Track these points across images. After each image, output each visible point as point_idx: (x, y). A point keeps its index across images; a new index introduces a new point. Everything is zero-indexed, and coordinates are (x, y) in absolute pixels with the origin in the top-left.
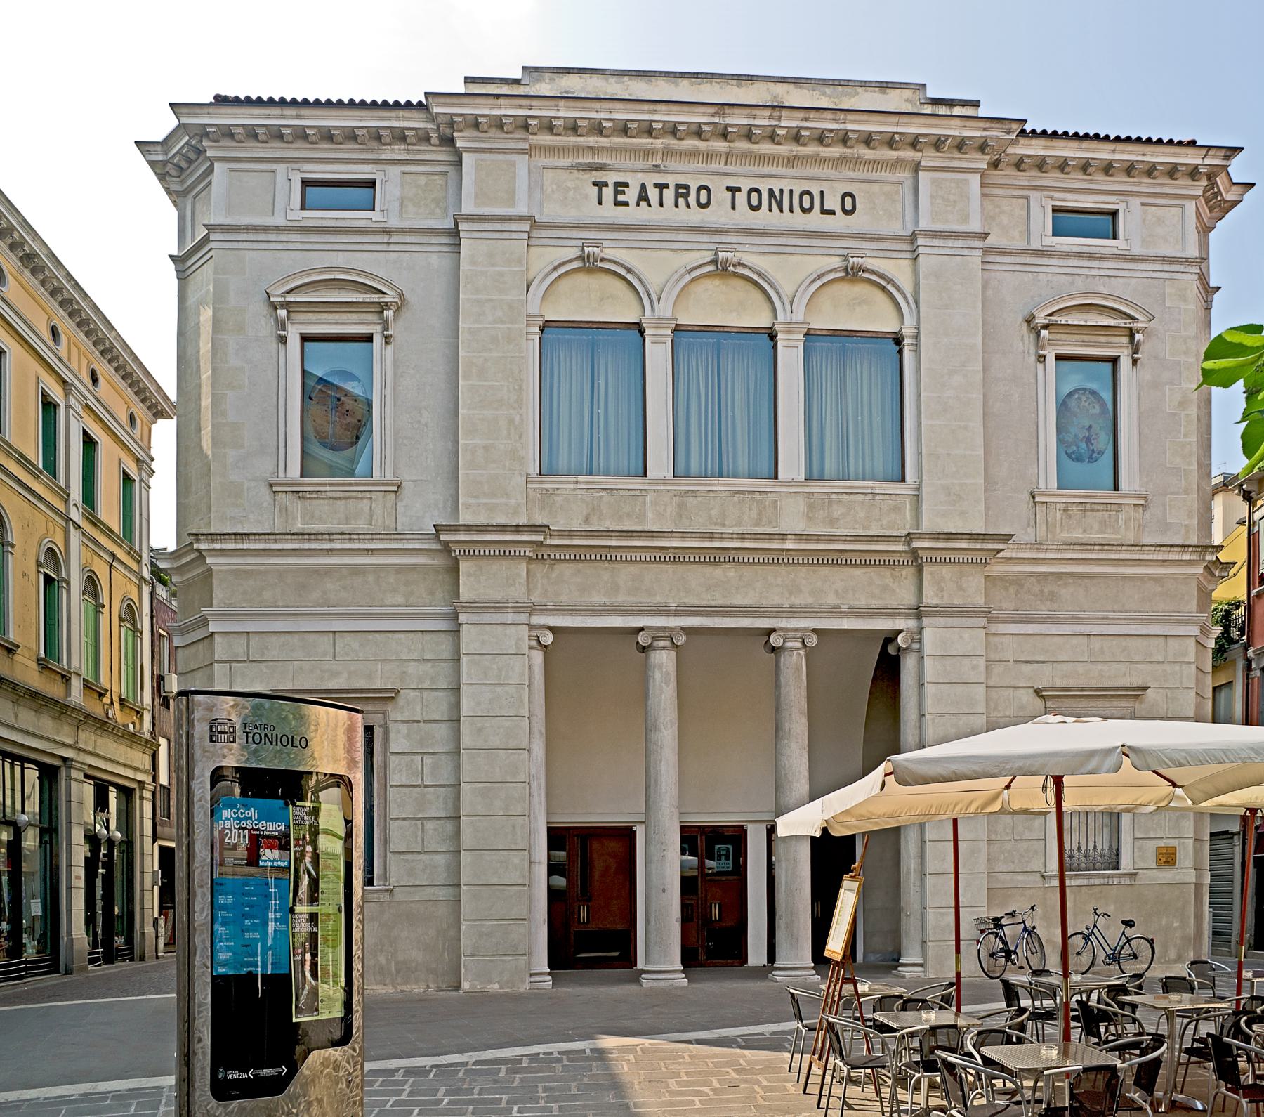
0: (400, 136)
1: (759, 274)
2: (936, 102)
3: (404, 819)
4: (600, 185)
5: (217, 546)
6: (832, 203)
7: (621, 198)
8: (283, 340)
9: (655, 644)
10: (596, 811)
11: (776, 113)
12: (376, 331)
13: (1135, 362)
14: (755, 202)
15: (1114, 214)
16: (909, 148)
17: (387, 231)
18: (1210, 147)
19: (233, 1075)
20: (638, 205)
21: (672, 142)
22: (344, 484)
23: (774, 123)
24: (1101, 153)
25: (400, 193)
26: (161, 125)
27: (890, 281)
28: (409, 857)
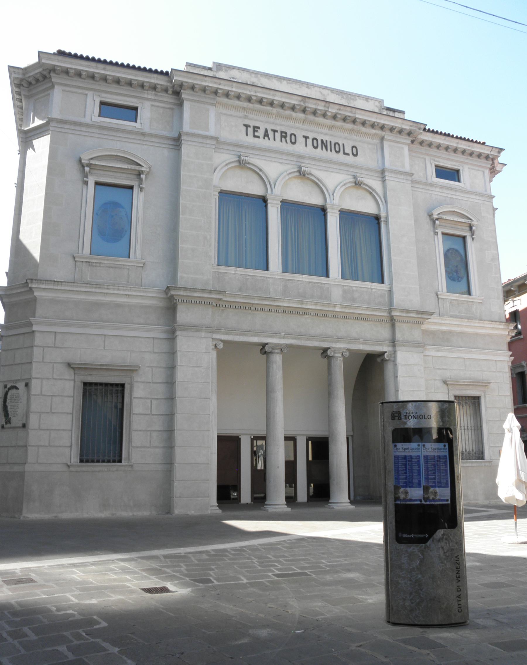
0: (154, 88)
1: (318, 180)
2: (388, 109)
3: (140, 431)
4: (247, 126)
5: (43, 286)
6: (348, 150)
7: (256, 134)
8: (86, 183)
9: (273, 351)
10: (230, 431)
11: (327, 105)
12: (135, 183)
13: (473, 239)
14: (315, 145)
15: (136, 109)
16: (361, 125)
17: (143, 134)
18: (493, 147)
19: (405, 536)
20: (264, 138)
21: (281, 111)
22: (114, 261)
23: (327, 109)
24: (453, 143)
25: (150, 114)
26: (27, 59)
27: (374, 190)
28: (143, 449)
